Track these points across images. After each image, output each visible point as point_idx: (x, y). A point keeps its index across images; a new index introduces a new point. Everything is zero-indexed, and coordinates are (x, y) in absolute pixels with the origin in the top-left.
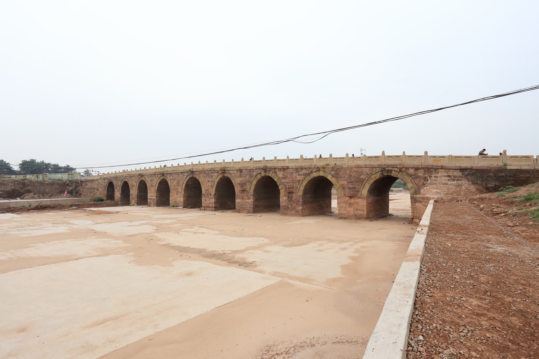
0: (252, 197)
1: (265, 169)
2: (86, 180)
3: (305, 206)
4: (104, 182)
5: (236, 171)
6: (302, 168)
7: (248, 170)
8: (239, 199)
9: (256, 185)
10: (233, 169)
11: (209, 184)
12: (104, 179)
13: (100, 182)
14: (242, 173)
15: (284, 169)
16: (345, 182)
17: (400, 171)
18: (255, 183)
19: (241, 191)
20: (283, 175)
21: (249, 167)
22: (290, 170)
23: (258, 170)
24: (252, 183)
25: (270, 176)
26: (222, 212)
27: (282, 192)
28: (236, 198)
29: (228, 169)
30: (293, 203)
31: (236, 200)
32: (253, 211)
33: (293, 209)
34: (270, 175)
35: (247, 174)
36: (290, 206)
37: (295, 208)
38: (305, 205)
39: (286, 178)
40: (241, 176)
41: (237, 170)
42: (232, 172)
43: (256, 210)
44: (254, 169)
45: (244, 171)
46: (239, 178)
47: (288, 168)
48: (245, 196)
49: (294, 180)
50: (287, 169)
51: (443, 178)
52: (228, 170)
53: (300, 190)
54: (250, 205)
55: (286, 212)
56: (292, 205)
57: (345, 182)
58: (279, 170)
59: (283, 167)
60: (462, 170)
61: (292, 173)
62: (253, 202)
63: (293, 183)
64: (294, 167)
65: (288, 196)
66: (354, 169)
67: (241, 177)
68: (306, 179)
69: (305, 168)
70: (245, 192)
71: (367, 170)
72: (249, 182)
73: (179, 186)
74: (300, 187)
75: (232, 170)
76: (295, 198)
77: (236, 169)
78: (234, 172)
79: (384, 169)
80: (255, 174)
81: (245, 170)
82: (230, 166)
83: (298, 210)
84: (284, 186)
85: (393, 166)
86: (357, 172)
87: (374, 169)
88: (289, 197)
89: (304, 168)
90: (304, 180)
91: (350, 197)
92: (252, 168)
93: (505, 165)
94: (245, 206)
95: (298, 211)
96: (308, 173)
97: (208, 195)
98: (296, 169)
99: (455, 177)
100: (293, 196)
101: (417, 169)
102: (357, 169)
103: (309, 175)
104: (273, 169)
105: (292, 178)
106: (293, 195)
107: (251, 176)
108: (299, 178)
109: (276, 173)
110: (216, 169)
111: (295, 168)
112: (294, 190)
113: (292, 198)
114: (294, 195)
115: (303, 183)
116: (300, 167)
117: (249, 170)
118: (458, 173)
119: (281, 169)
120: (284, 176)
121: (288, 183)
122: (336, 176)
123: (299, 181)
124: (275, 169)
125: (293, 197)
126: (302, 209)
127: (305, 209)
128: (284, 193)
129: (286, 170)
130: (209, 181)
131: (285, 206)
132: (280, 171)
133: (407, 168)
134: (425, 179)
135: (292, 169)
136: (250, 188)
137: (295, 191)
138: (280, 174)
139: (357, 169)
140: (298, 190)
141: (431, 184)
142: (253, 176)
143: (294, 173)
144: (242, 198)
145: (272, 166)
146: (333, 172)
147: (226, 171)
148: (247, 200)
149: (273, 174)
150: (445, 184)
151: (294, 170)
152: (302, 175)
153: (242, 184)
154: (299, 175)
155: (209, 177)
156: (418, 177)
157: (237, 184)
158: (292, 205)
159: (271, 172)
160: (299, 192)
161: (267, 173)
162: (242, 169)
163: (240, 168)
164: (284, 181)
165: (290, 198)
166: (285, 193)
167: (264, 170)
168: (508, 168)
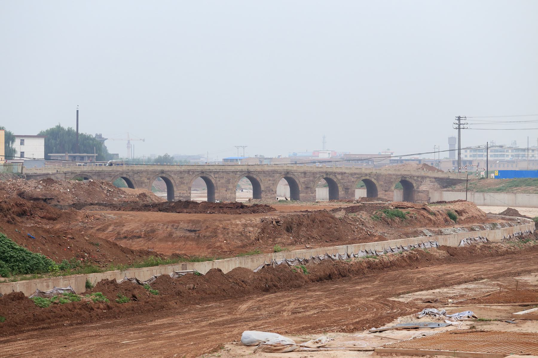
2: (36, 174)
4: (65, 178)
6: (355, 174)
8: (303, 194)
10: (298, 171)
11: (270, 182)
12: (65, 173)
13: (58, 177)
15: (342, 174)
16: (383, 183)
17: (411, 178)
20: (342, 177)
23: (320, 174)
27: (340, 189)
35: (311, 176)
40: (305, 177)
41: (301, 173)
42: (296, 174)
47: (345, 173)
50: (345, 173)
51: (428, 182)
56: (348, 197)
57: (383, 183)
59: (341, 172)
60: (435, 178)
66: (387, 176)
71: (394, 177)
72: (313, 181)
73: (229, 183)
79: (403, 176)
80: (318, 176)
82: (292, 169)
85: (407, 175)
86: (389, 177)
87: (398, 176)
88: (346, 191)
91: (386, 191)
93: (449, 177)
94: (309, 199)
97: (269, 191)
99: (433, 181)
101: (418, 177)
102: (389, 176)
107: (314, 177)
108: (353, 180)
109: (335, 176)
110: (279, 171)
112: (349, 187)
113: (348, 192)
114: (350, 190)
118: (434, 180)
119: (339, 174)
121: (345, 182)
122: (377, 179)
123: (353, 182)
130: (270, 180)
133: (414, 177)
134: (421, 182)
138: (339, 177)
139: (389, 176)
141: (424, 184)
142: (316, 177)
144: (306, 193)
146: (375, 177)
150: (429, 184)
154: (354, 178)
155: (270, 177)
156: (418, 181)
158: (348, 197)
164: (342, 181)
166: (343, 189)
168: (450, 178)
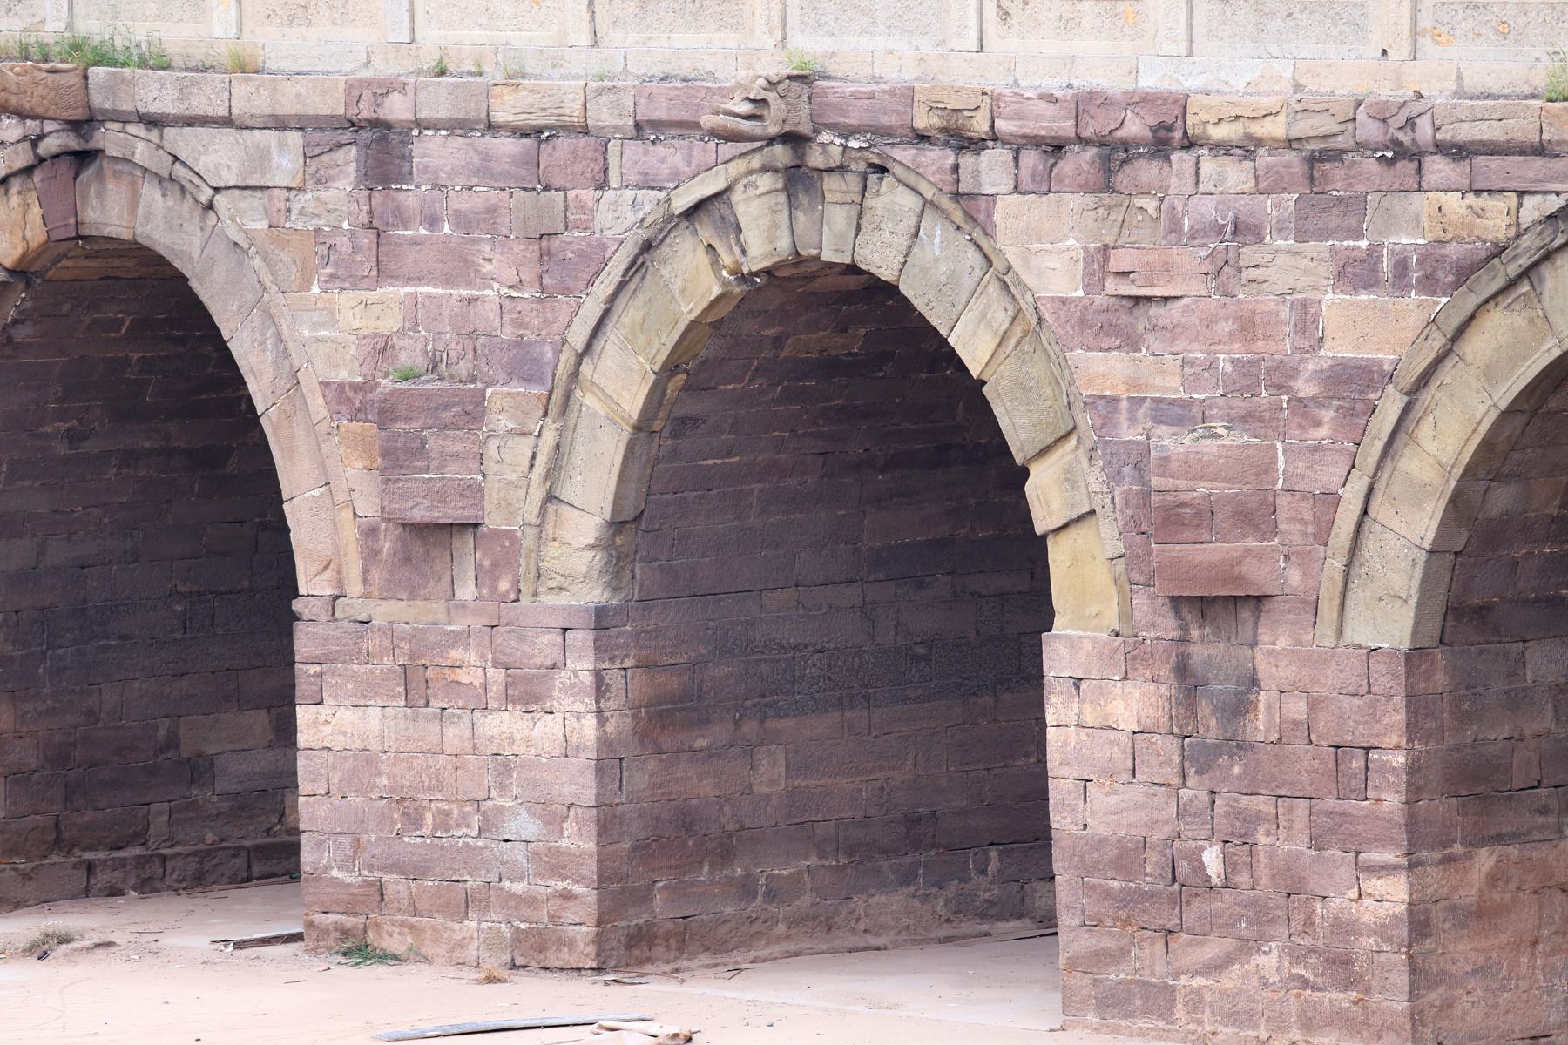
0: (581, 667)
1: (793, 139)
3: (1485, 859)
5: (294, 138)
7: (507, 146)
9: (642, 427)
10: (248, 98)
14: (410, 197)
18: (633, 402)
19: (386, 545)
20: (1098, 261)
21: (514, 79)
22: (1209, 166)
23: (669, 156)
24: (588, 401)
25: (886, 274)
26: (40, 950)
28: (305, 672)
29: (156, 95)
30: (1262, 804)
31: (304, 714)
32: (599, 941)
33: (1262, 915)
34: (880, 259)
36: (1212, 859)
37: (1293, 889)
38: (1499, 839)
39: (1141, 321)
43: (662, 909)
44: (603, 115)
45: (431, 152)
46: (345, 278)
48: (462, 639)
49: (1281, 378)
52: (154, 122)
53: (1370, 545)
54: (554, 821)
55: (1150, 962)
56: (1239, 840)
58: (1030, 158)
59: (1084, 103)
61: (1244, 230)
62: (609, 761)
63: (1247, 419)
64: (1275, 128)
65: (1183, 670)
67: (383, 272)
68: (1478, 345)
69: (1458, 151)
70: (468, 554)
72: (523, 364)
74: (1378, 509)
75: (227, 122)
76: (1296, 708)
77: (288, 107)
78: (262, 158)
81: (459, 127)
83: (1345, 928)
84: (1115, 478)
89: (1441, 148)
90: (1446, 374)
92: (572, 111)
94: (465, 835)
95: (1346, 961)
96: (1499, 251)
98: (1314, 160)
100: (1264, 669)
103: (1525, 274)
104: (922, 138)
105: (1247, 327)
106: (1254, 644)
111: (1290, 143)
113: (1239, 707)
115: (1425, 432)
116: (1369, 130)
117: (522, 133)
119: (1056, 148)
120: (1113, 286)
124: (967, 143)
125: (1254, 682)
126: (1419, 922)
127: (1481, 916)
128: (1111, 618)
129: (1147, 171)
131: (1127, 857)
132: (1045, 185)
135: (1247, 148)
136: (550, 498)
137: (1294, 577)
140: (1337, 564)
143: (1281, 230)
145: (909, 74)
147: (110, 139)
148: (502, 725)
149: (936, 234)
151: (1269, 186)
152: (1402, 267)
153: (386, 413)
157: (317, 404)
158: (1239, 840)
159: (892, 200)
160: (1357, 596)
161: (839, 218)
162: (397, 109)
163: (354, 90)
165: (1204, 708)
166: (1127, 611)
167: (781, 154)
